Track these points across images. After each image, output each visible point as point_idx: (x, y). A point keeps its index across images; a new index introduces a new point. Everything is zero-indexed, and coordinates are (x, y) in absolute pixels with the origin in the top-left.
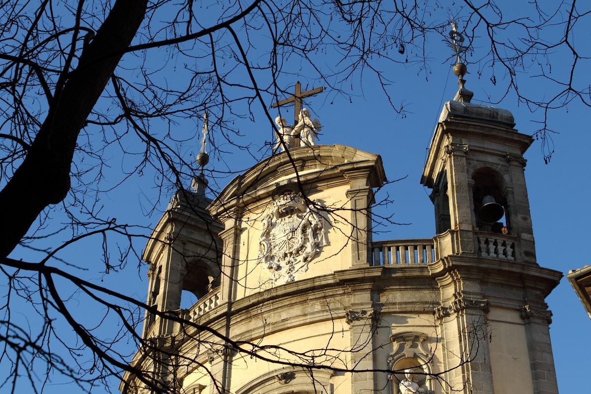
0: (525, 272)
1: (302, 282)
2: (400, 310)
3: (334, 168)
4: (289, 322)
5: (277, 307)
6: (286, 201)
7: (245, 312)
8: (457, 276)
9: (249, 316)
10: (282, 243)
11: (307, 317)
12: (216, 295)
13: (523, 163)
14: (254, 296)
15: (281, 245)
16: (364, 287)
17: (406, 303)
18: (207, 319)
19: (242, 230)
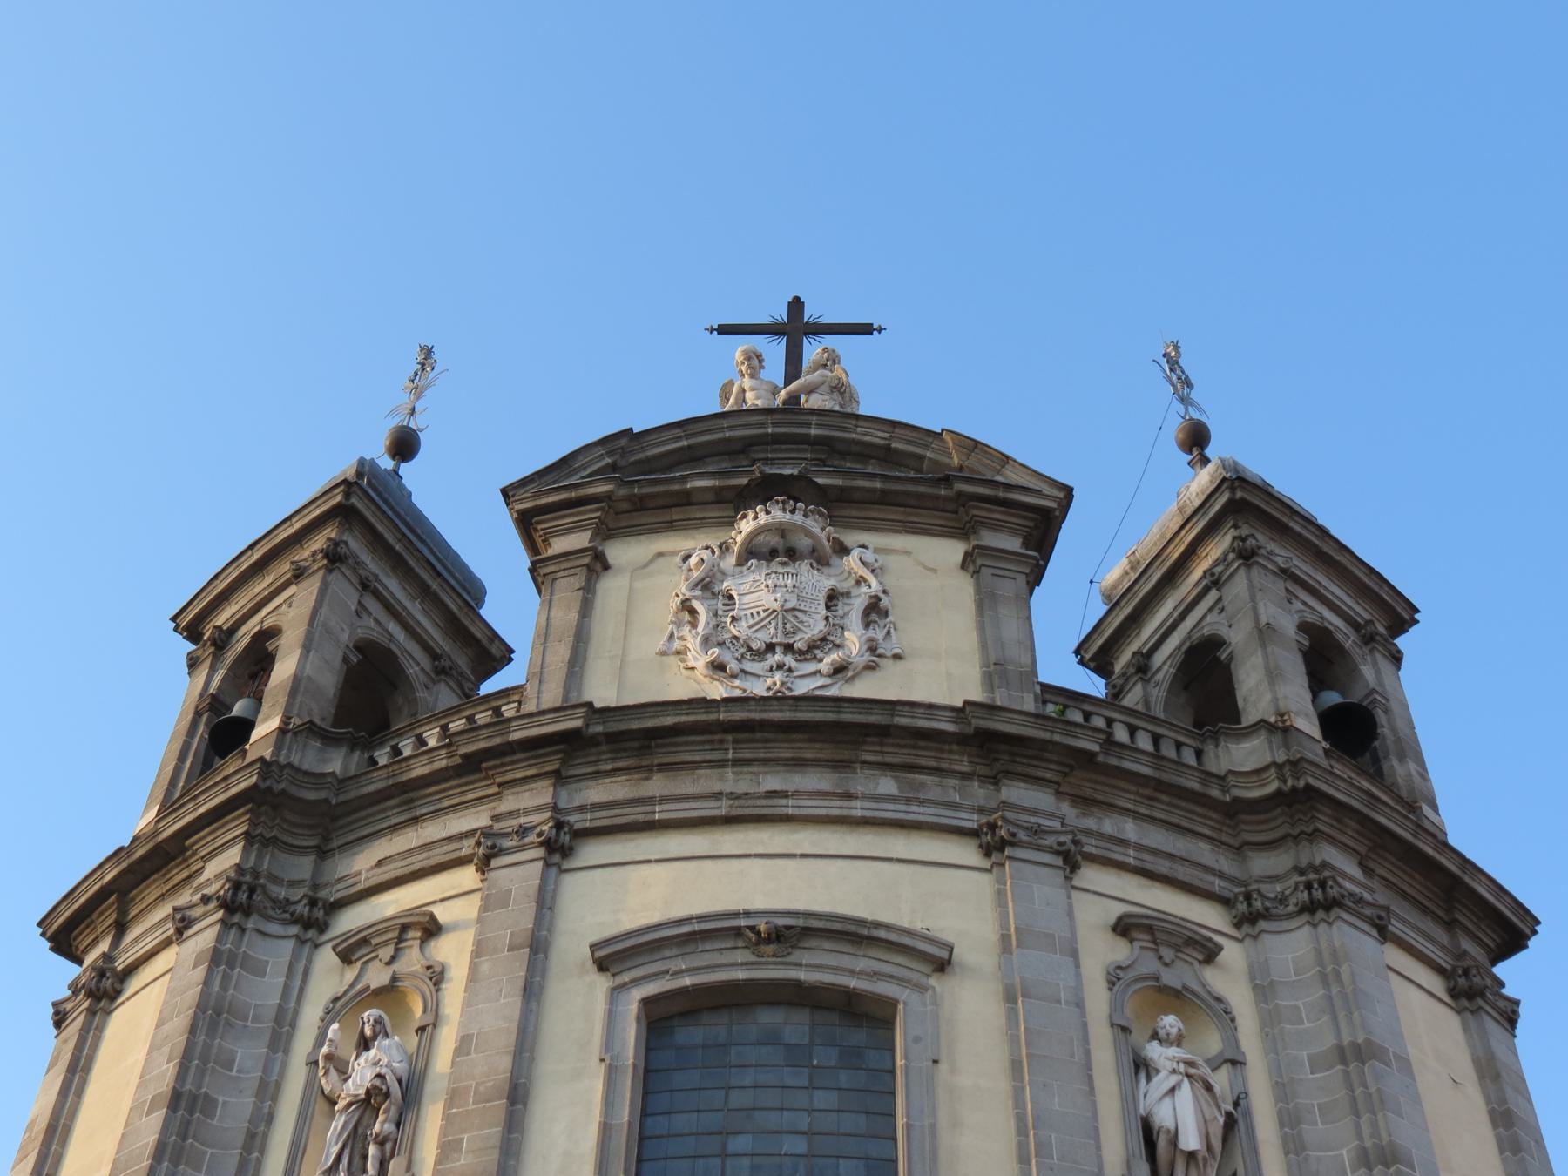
0: (1467, 879)
1: (855, 705)
2: (1139, 864)
3: (940, 479)
4: (791, 802)
9: (645, 763)
10: (763, 615)
11: (853, 804)
13: (1397, 658)
15: (757, 619)
16: (1040, 773)
17: (1155, 852)
18: (497, 741)
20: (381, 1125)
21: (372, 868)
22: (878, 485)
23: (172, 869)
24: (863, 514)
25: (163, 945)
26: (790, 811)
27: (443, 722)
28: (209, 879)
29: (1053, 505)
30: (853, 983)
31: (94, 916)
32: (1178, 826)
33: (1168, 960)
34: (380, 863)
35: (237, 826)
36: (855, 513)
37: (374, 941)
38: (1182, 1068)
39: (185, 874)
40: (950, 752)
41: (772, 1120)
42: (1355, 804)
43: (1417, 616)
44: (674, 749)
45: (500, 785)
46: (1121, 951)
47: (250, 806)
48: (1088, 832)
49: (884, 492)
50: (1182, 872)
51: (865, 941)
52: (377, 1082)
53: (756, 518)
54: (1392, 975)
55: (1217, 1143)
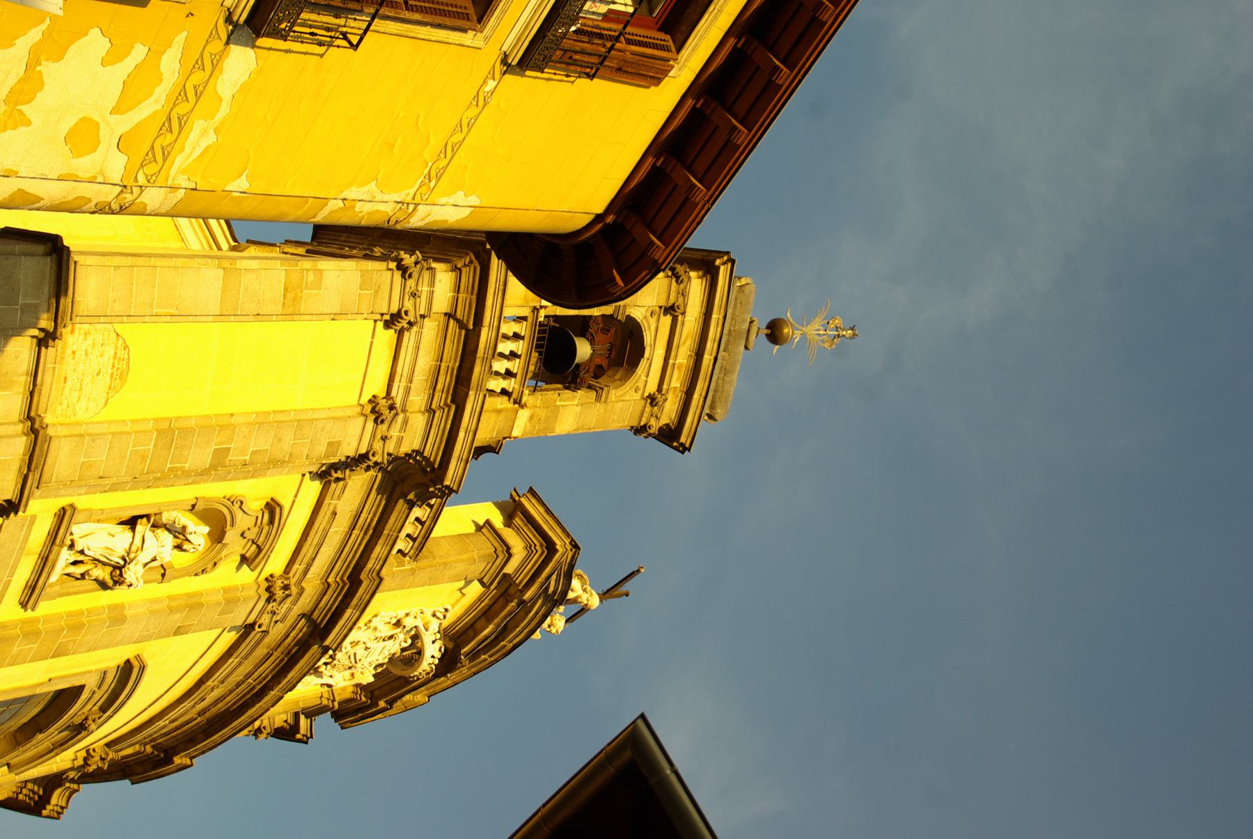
7: (291, 650)
12: (414, 540)
14: (295, 682)
21: (335, 508)
23: (451, 379)
25: (393, 372)
27: (435, 508)
28: (405, 431)
31: (474, 297)
34: (334, 514)
35: (432, 451)
37: (265, 531)
39: (439, 387)
44: (275, 663)
47: (436, 466)
51: (52, 747)
53: (433, 657)
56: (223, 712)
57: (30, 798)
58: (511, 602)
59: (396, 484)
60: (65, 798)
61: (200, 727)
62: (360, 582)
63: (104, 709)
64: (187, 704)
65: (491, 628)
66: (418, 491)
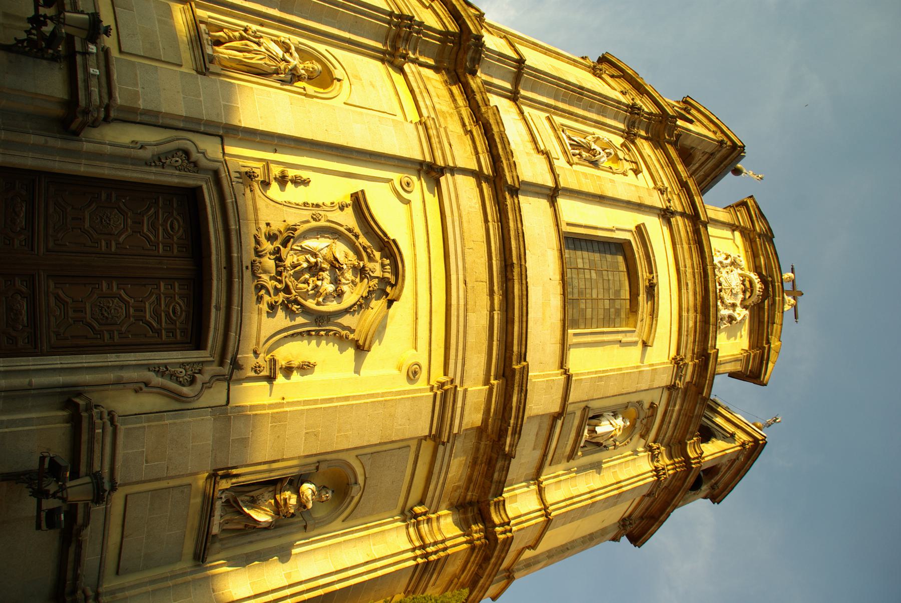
4: (685, 291)
5: (696, 277)
6: (758, 289)
8: (679, 467)
9: (691, 242)
18: (693, 192)
19: (733, 231)
20: (585, 154)
22: (766, 319)
24: (755, 316)
26: (683, 291)
29: (762, 380)
30: (640, 312)
32: (677, 424)
33: (643, 421)
34: (649, 156)
36: (755, 313)
38: (618, 427)
40: (701, 345)
41: (600, 285)
42: (686, 484)
43: (716, 504)
45: (678, 194)
46: (646, 405)
48: (678, 394)
49: (763, 322)
50: (665, 427)
52: (598, 152)
54: (632, 500)
55: (594, 441)
56: (702, 302)
57: (682, 467)
58: (756, 238)
59: (658, 142)
60: (694, 453)
61: (703, 321)
62: (686, 181)
63: (651, 272)
64: (684, 291)
65: (762, 258)
66: (666, 131)
